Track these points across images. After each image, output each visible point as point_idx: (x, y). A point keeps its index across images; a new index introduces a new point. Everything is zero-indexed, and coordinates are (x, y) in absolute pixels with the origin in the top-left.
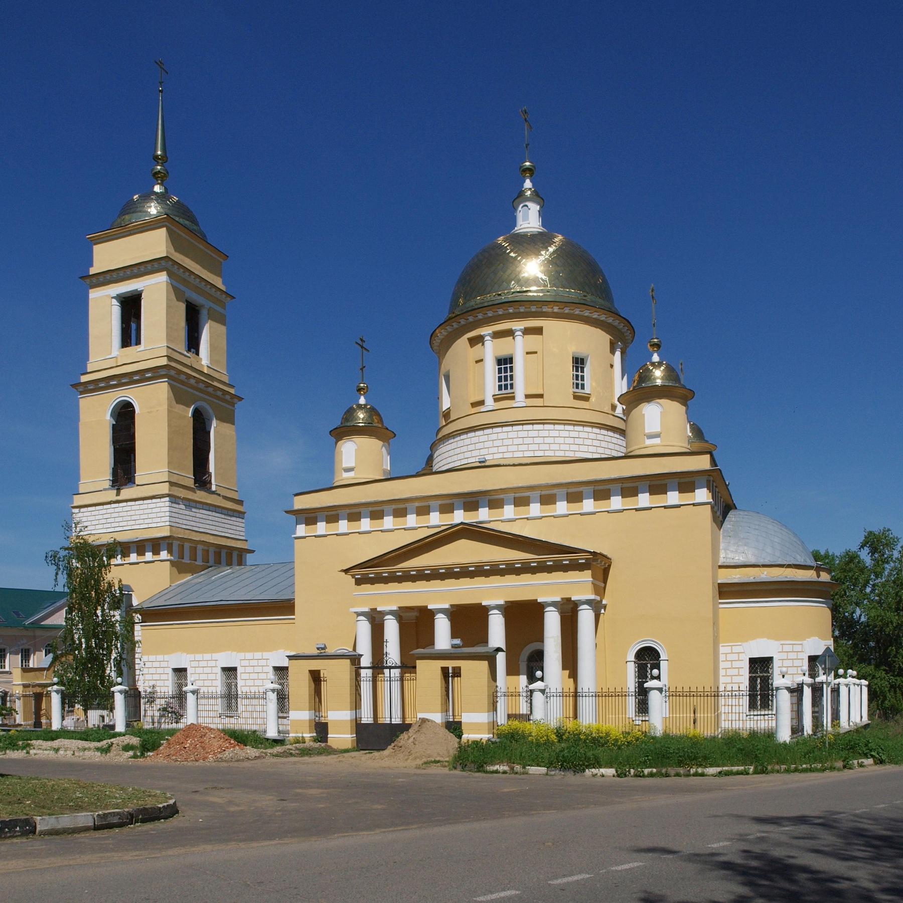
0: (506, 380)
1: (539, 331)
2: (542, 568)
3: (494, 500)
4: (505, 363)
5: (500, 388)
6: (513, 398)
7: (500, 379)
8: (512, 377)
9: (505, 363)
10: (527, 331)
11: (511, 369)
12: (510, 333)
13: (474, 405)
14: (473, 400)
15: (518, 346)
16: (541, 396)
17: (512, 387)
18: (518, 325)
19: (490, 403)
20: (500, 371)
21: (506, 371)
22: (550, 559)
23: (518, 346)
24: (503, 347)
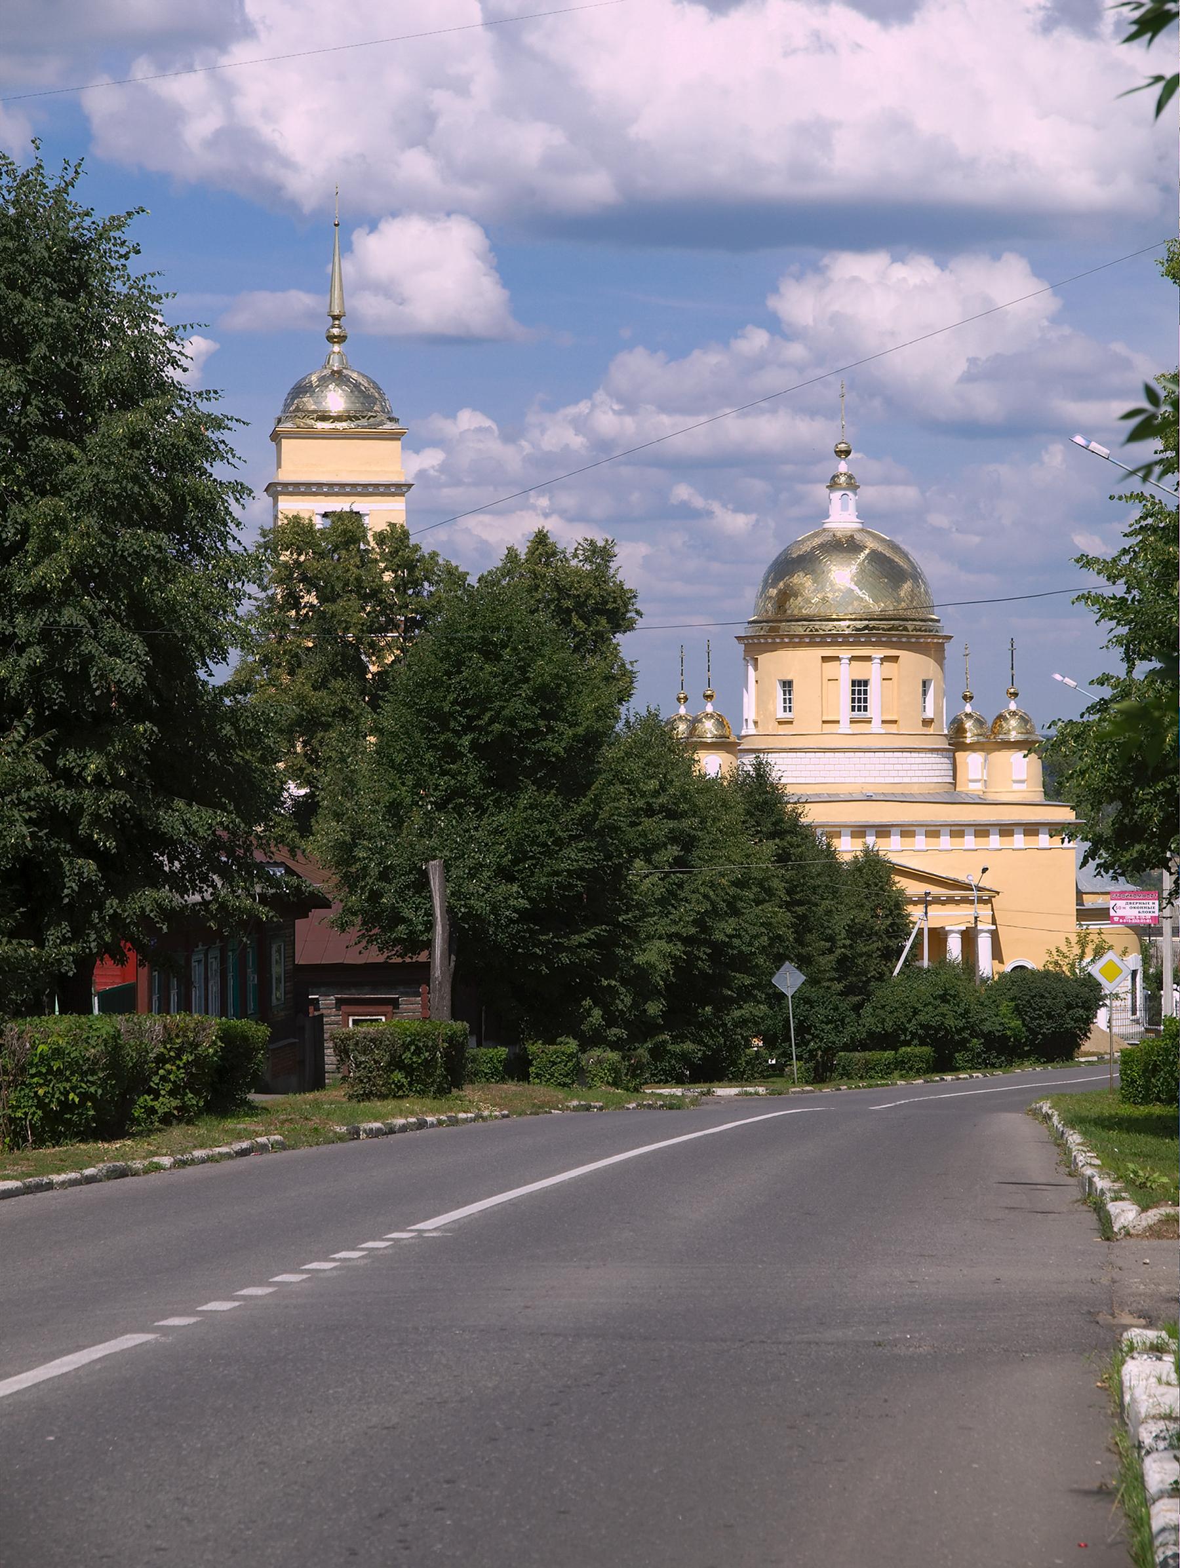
0: (859, 701)
1: (895, 659)
2: (950, 900)
3: (883, 831)
4: (859, 685)
5: (853, 710)
6: (868, 721)
7: (853, 700)
8: (866, 700)
9: (859, 685)
10: (885, 659)
11: (866, 692)
12: (868, 659)
13: (824, 722)
14: (825, 718)
15: (874, 672)
16: (895, 722)
17: (865, 709)
18: (878, 653)
19: (845, 727)
20: (853, 692)
21: (859, 693)
22: (958, 894)
23: (874, 672)
24: (859, 671)
